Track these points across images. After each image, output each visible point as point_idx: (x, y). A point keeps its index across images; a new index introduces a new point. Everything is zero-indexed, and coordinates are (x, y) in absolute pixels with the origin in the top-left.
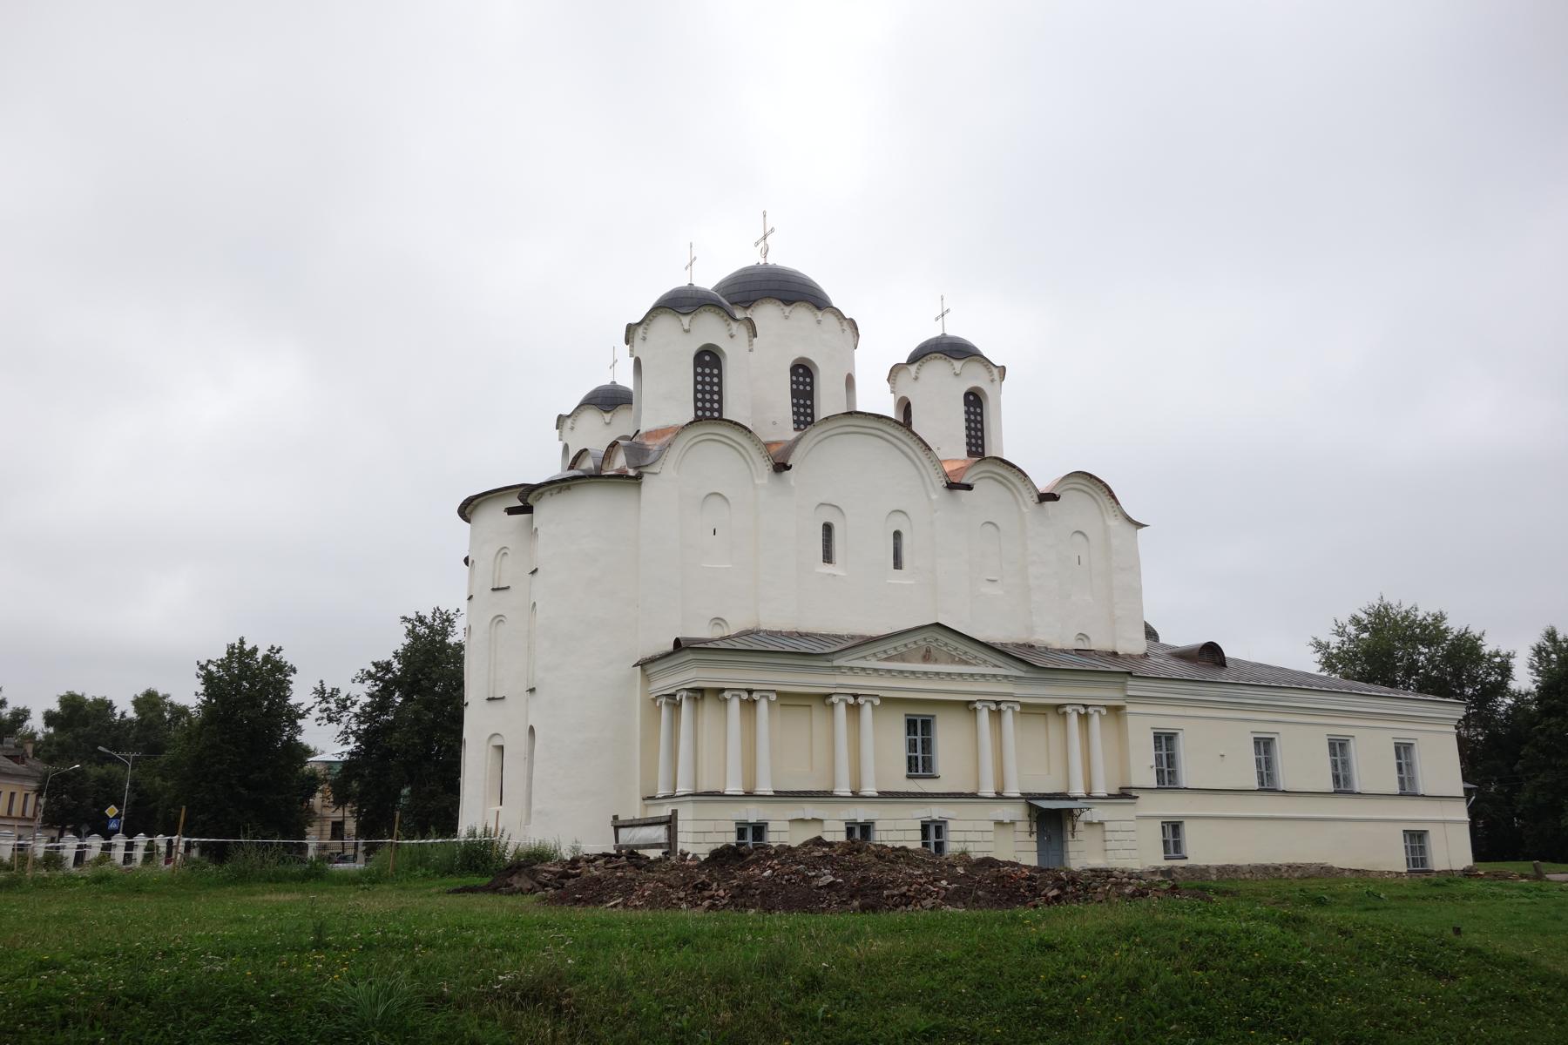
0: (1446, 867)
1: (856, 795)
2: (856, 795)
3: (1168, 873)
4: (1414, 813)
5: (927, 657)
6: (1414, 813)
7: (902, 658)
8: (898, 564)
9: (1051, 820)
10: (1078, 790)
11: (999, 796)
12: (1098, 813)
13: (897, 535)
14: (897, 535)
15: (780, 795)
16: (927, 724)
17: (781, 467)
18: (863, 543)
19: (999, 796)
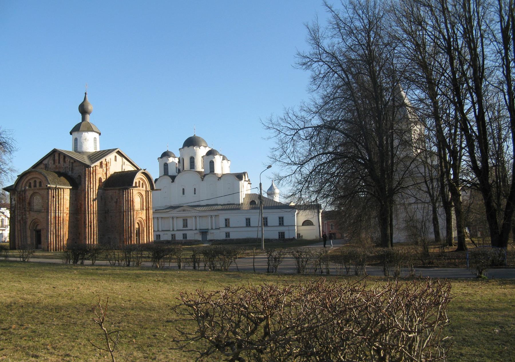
0: (288, 238)
1: (173, 230)
2: (173, 230)
3: (225, 240)
4: (281, 229)
5: (184, 211)
6: (281, 229)
7: (180, 211)
8: (195, 194)
9: (204, 233)
10: (210, 228)
11: (196, 229)
12: (212, 231)
13: (195, 189)
14: (195, 189)
15: (162, 231)
16: (187, 220)
17: (173, 181)
18: (189, 191)
19: (196, 229)
